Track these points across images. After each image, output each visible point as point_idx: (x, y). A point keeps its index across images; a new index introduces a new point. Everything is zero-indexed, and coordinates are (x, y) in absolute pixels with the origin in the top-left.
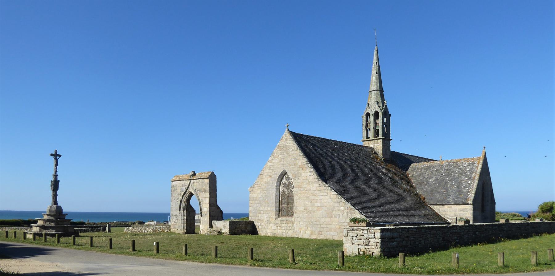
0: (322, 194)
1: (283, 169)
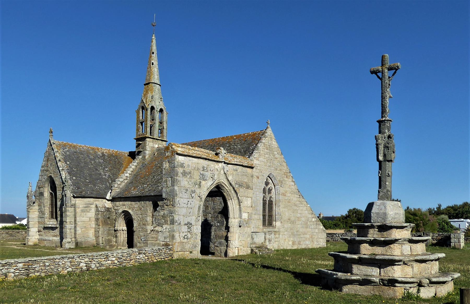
0: (301, 205)
1: (270, 172)
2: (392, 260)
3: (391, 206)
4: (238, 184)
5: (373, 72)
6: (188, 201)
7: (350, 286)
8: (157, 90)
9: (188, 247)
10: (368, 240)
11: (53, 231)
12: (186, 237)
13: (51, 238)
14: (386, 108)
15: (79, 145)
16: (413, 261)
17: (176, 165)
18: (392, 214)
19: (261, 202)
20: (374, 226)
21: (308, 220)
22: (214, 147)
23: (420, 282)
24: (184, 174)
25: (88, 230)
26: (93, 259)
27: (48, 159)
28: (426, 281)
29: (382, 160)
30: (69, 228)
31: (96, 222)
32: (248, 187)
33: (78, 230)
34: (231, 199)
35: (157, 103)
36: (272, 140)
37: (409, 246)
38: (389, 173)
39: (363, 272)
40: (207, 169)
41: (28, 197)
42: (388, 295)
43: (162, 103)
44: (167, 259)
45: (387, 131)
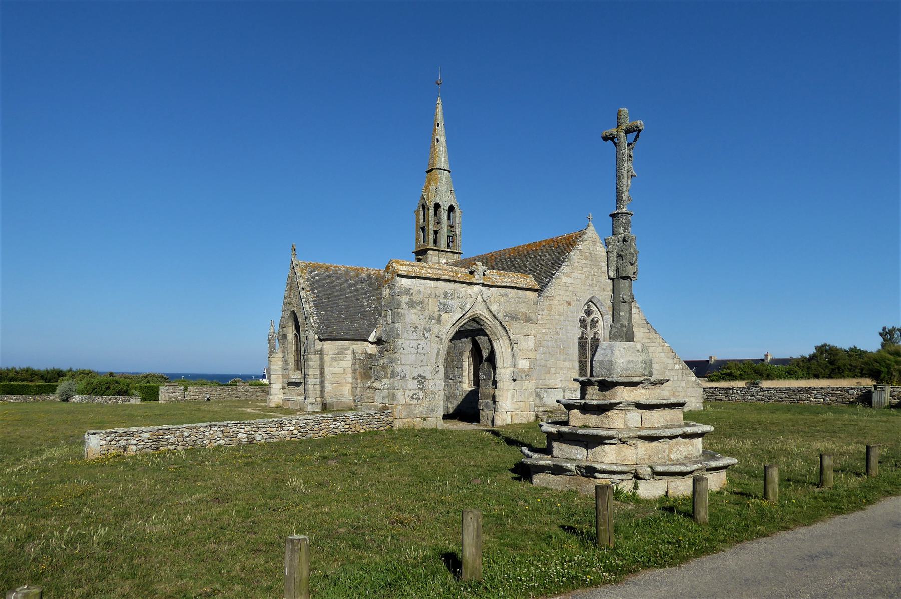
0: (653, 345)
2: (597, 435)
3: (622, 349)
5: (605, 138)
6: (420, 344)
7: (540, 476)
8: (444, 179)
9: (419, 411)
10: (578, 404)
11: (298, 388)
12: (415, 397)
13: (295, 398)
14: (622, 194)
15: (335, 265)
16: (635, 438)
17: (397, 291)
18: (623, 363)
19: (575, 342)
20: (592, 382)
21: (665, 368)
22: (516, 259)
23: (635, 472)
24: (412, 304)
25: (342, 386)
26: (258, 428)
27: (291, 286)
28: (645, 471)
29: (614, 276)
30: (313, 384)
31: (353, 375)
32: (528, 320)
33: (328, 387)
34: (498, 339)
35: (445, 198)
36: (595, 245)
37: (638, 414)
38: (624, 297)
39: (566, 454)
40: (452, 295)
41: (269, 340)
42: (588, 492)
43: (452, 197)
44: (383, 428)
45: (621, 230)
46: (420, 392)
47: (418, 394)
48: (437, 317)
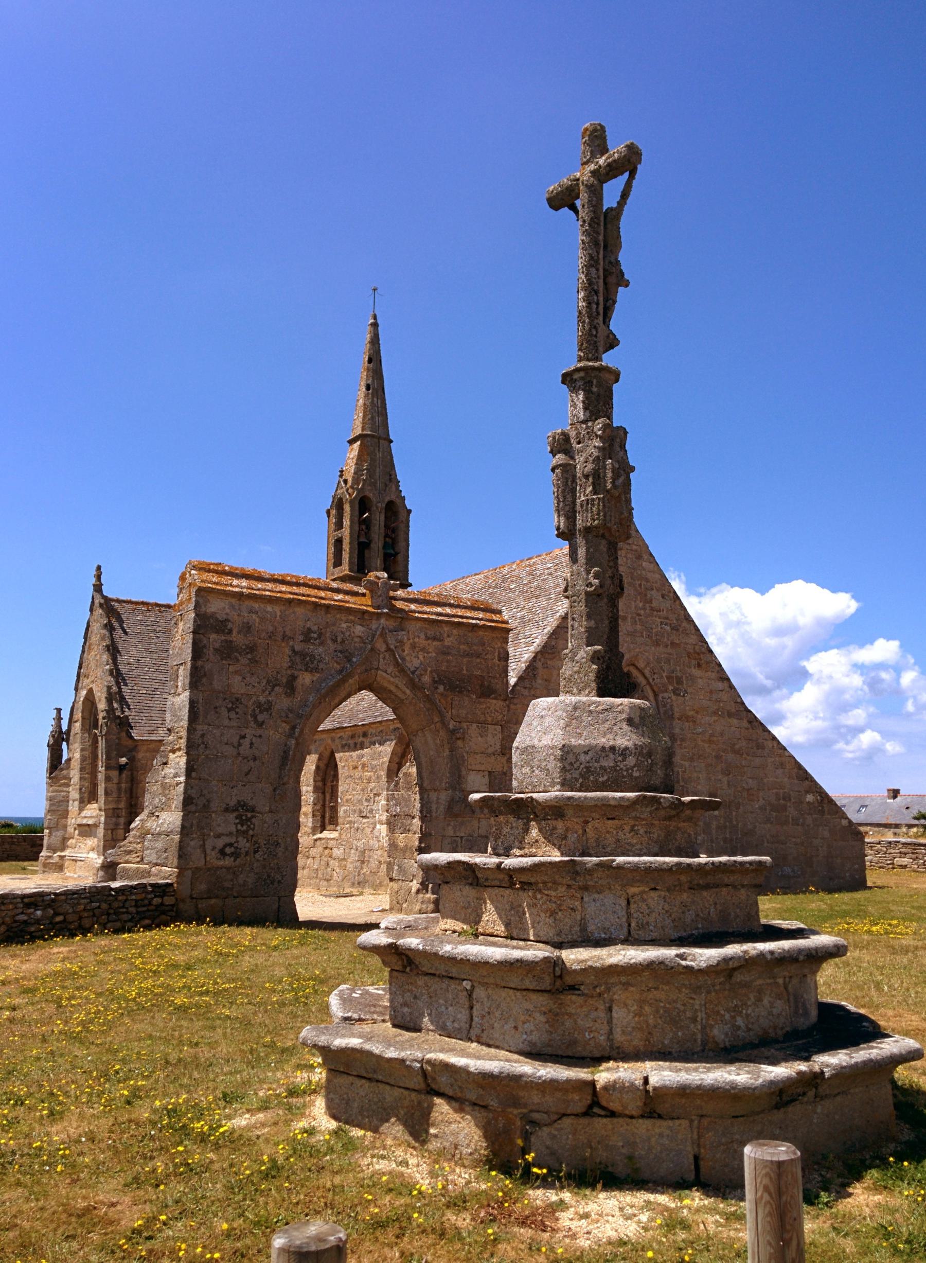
4: (444, 684)
6: (244, 737)
12: (228, 850)
46: (240, 839)
47: (236, 845)
48: (284, 680)
